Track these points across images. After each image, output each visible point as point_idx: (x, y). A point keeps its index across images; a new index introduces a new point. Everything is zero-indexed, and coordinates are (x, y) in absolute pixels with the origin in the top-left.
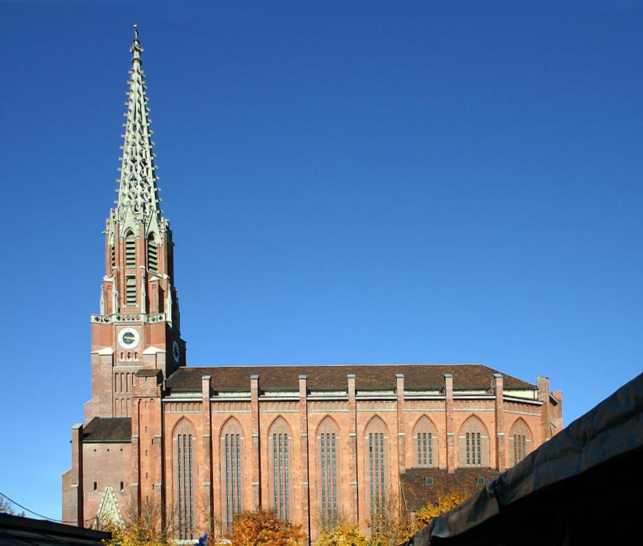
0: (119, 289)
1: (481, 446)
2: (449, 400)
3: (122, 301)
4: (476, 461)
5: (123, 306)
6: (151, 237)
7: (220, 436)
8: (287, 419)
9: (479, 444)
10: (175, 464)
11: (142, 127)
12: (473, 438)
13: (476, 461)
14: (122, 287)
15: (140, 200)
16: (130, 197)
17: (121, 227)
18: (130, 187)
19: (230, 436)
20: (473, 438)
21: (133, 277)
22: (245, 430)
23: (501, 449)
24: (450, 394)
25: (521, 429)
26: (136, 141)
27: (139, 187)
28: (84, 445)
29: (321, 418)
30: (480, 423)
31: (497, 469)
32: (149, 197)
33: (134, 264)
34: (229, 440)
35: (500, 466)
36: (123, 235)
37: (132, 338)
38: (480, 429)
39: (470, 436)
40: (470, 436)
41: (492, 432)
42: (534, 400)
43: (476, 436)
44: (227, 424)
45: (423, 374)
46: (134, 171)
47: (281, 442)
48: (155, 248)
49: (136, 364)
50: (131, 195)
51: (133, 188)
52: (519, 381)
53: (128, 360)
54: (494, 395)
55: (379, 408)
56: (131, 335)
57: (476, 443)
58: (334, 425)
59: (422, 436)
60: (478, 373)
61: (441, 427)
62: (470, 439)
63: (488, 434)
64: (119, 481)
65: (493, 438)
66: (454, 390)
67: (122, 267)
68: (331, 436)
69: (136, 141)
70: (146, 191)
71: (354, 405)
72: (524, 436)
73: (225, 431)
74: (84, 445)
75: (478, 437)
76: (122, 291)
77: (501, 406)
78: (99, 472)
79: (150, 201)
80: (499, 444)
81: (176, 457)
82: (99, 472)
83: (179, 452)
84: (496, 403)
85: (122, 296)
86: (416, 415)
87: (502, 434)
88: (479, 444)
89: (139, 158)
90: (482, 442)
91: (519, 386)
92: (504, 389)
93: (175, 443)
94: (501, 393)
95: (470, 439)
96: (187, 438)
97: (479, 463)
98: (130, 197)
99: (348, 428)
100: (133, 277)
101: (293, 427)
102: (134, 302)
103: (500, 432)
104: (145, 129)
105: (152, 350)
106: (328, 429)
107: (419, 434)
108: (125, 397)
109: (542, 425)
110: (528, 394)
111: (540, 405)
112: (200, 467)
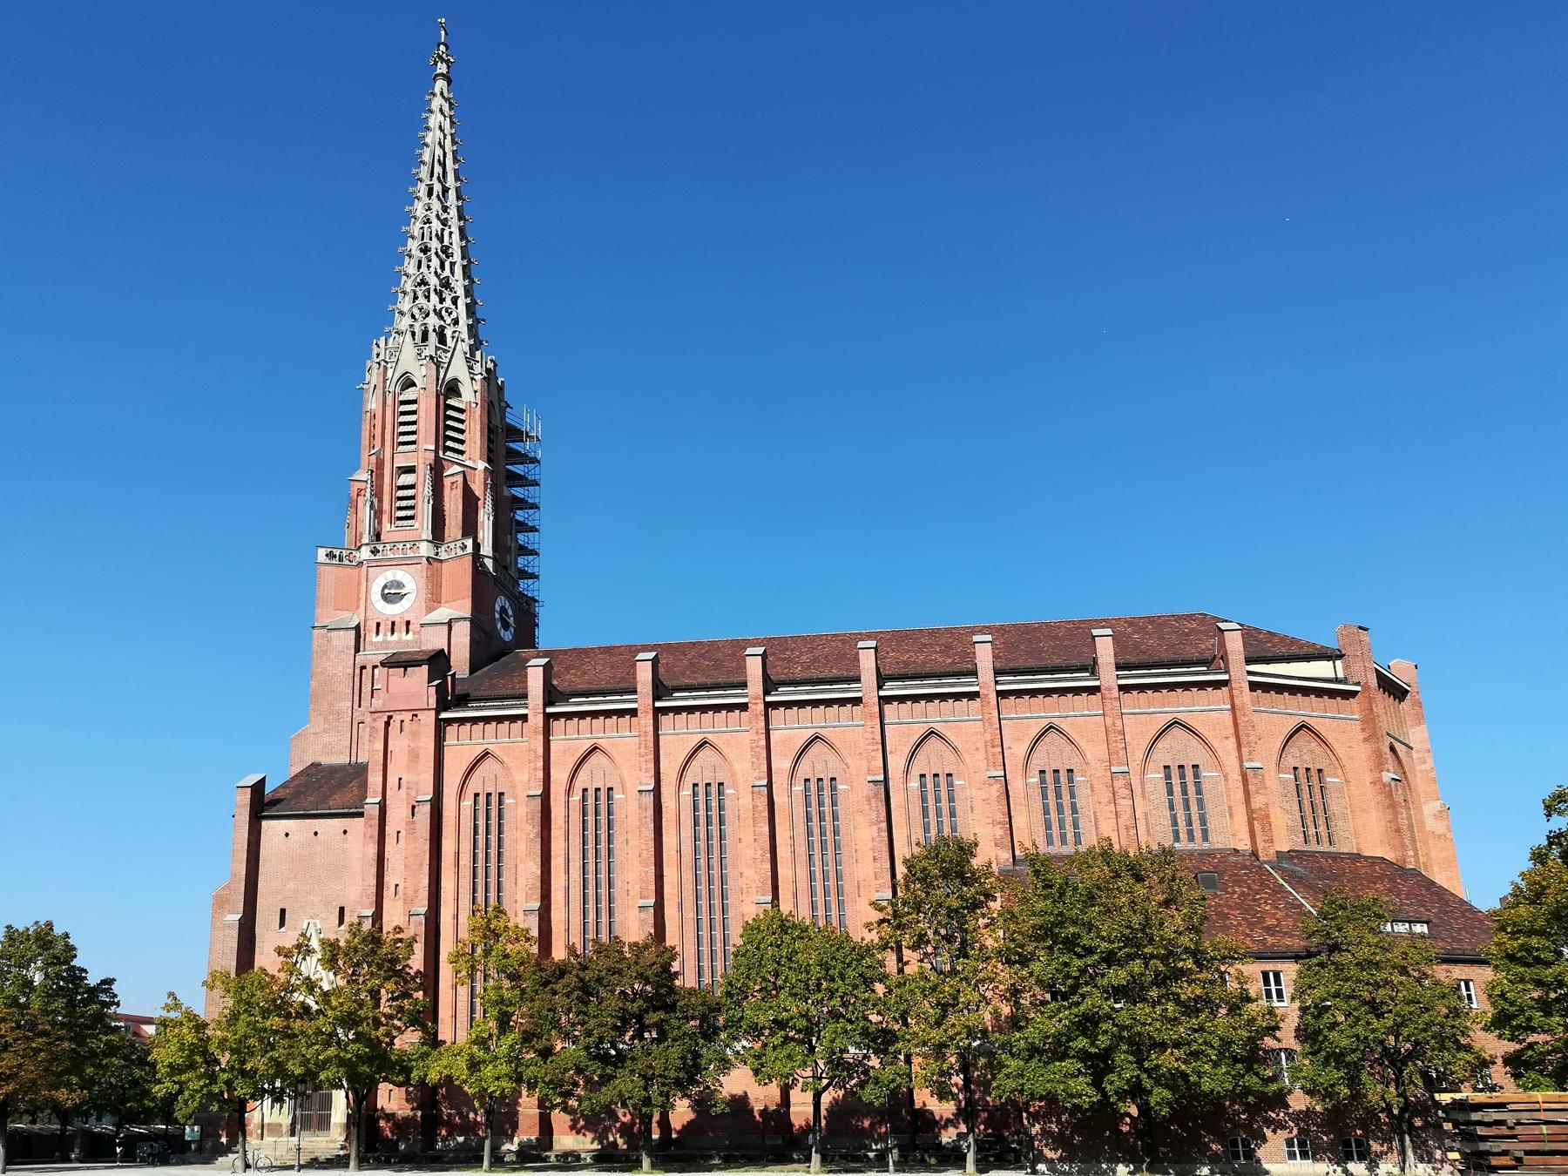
1: (1206, 796)
2: (1110, 689)
4: (1198, 834)
5: (386, 526)
6: (453, 389)
7: (569, 792)
8: (725, 751)
9: (1199, 792)
11: (445, 190)
12: (1182, 776)
13: (1198, 834)
15: (433, 321)
16: (413, 316)
18: (416, 298)
19: (591, 793)
20: (1182, 776)
21: (411, 470)
22: (627, 778)
23: (1258, 801)
24: (1108, 676)
25: (1305, 753)
26: (429, 215)
27: (434, 298)
28: (265, 823)
29: (800, 743)
30: (1194, 742)
31: (1254, 854)
32: (454, 315)
33: (413, 443)
34: (591, 801)
35: (1260, 845)
37: (403, 591)
38: (1192, 752)
39: (1175, 774)
40: (1175, 774)
41: (1231, 760)
42: (1337, 680)
43: (1189, 773)
44: (586, 766)
45: (1056, 638)
46: (424, 269)
47: (710, 804)
48: (462, 411)
50: (416, 311)
51: (422, 300)
52: (1294, 641)
54: (1227, 672)
55: (934, 714)
57: (1191, 790)
58: (831, 757)
59: (1049, 777)
60: (1192, 630)
61: (1095, 751)
62: (1176, 781)
63: (1220, 765)
65: (1235, 775)
66: (1118, 667)
67: (388, 450)
68: (826, 783)
69: (429, 215)
70: (448, 303)
71: (877, 709)
72: (1320, 771)
73: (582, 780)
74: (265, 823)
75: (1196, 776)
77: (1245, 697)
79: (456, 322)
80: (1252, 788)
84: (1231, 691)
86: (1029, 726)
87: (1258, 765)
88: (1199, 792)
89: (435, 245)
90: (1205, 786)
91: (1294, 650)
92: (1249, 661)
94: (1240, 672)
95: (1176, 781)
97: (1205, 838)
98: (413, 316)
99: (864, 764)
100: (411, 470)
101: (738, 766)
102: (412, 518)
103: (1251, 760)
104: (452, 194)
106: (819, 767)
107: (1042, 772)
109: (1365, 740)
110: (1322, 669)
111: (1354, 694)
112: (521, 867)
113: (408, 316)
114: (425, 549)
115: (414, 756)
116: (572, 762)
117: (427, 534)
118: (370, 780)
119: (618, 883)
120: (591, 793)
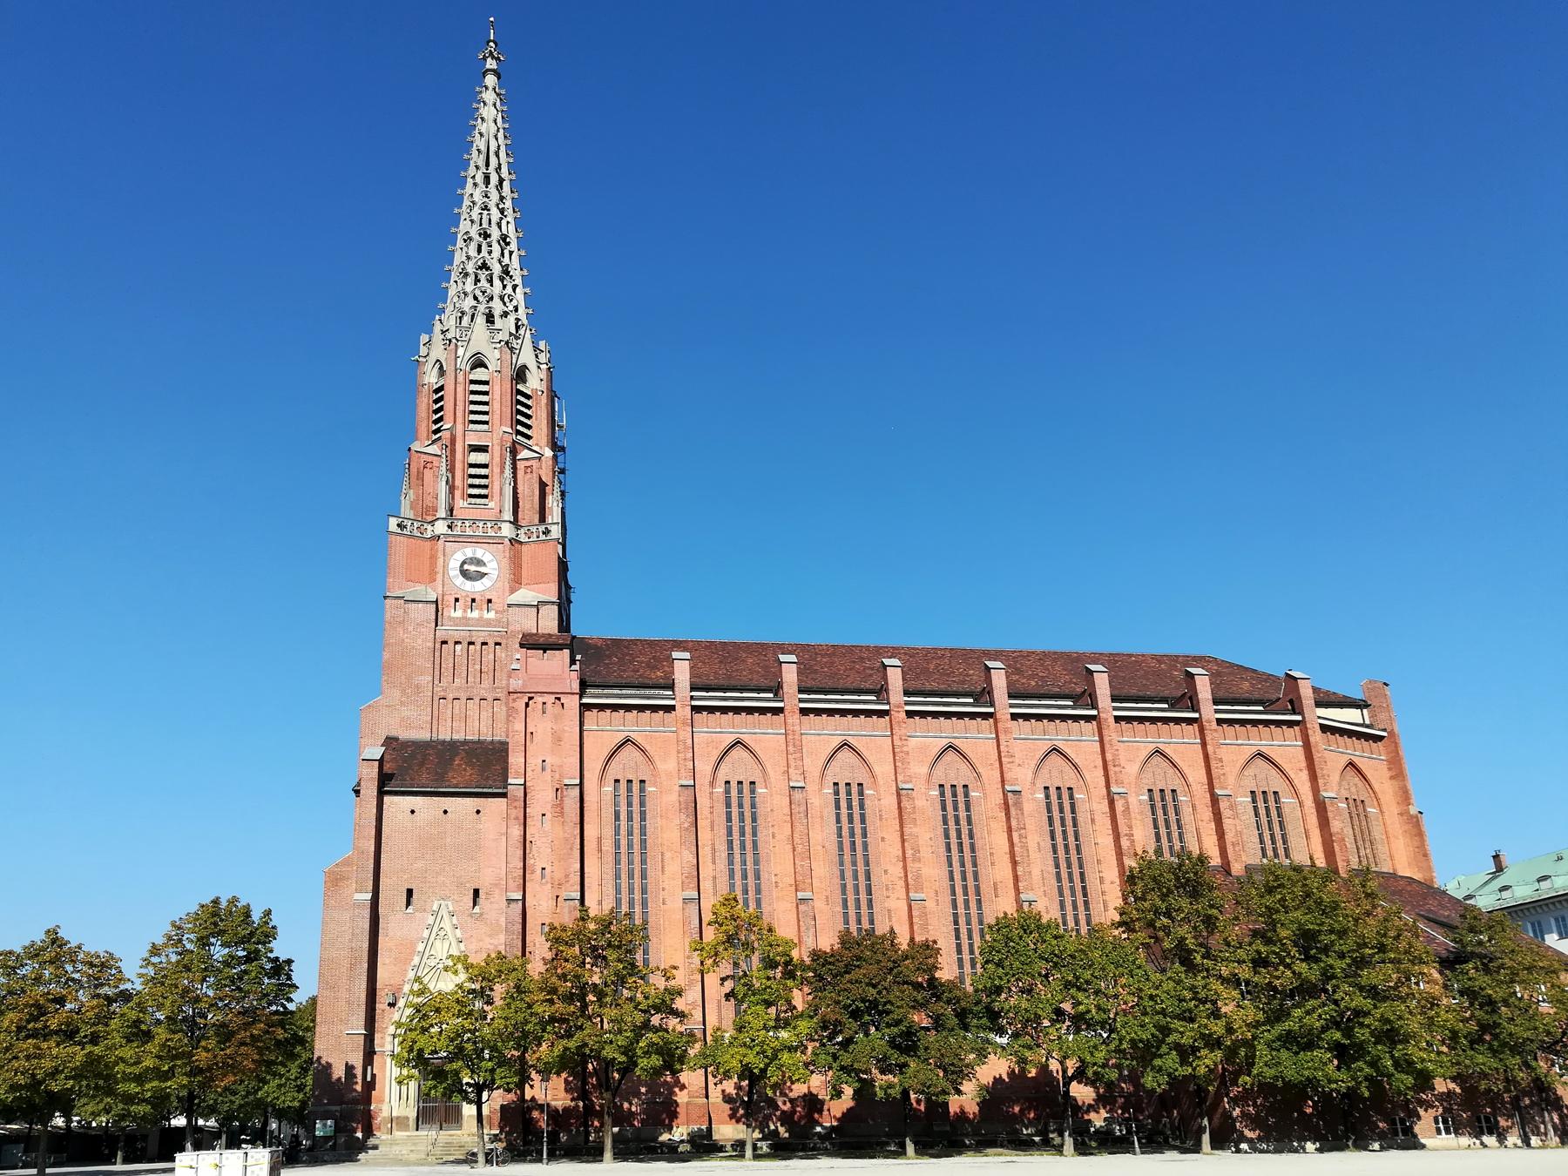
0: (451, 469)
3: (458, 493)
5: (460, 503)
10: (608, 846)
14: (458, 466)
17: (461, 352)
33: (486, 423)
36: (464, 365)
37: (482, 569)
49: (488, 623)
53: (469, 614)
56: (479, 562)
64: (471, 887)
67: (459, 427)
76: (458, 474)
78: (420, 864)
81: (609, 832)
82: (420, 864)
83: (617, 817)
85: (458, 482)
93: (609, 798)
96: (636, 787)
102: (485, 497)
105: (525, 595)
108: (451, 696)
113: (471, 297)
114: (507, 530)
115: (557, 739)
116: (716, 754)
117: (508, 516)
118: (511, 760)
119: (764, 876)
120: (734, 785)
